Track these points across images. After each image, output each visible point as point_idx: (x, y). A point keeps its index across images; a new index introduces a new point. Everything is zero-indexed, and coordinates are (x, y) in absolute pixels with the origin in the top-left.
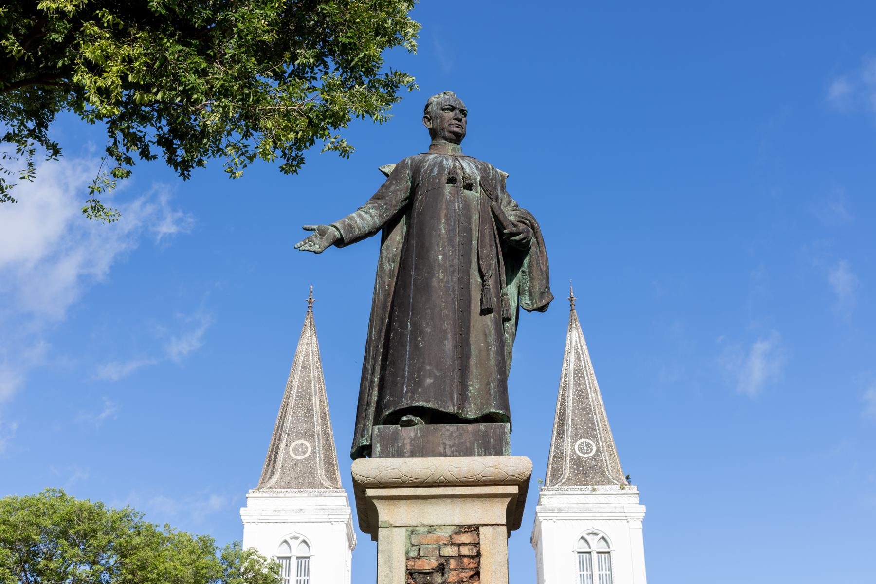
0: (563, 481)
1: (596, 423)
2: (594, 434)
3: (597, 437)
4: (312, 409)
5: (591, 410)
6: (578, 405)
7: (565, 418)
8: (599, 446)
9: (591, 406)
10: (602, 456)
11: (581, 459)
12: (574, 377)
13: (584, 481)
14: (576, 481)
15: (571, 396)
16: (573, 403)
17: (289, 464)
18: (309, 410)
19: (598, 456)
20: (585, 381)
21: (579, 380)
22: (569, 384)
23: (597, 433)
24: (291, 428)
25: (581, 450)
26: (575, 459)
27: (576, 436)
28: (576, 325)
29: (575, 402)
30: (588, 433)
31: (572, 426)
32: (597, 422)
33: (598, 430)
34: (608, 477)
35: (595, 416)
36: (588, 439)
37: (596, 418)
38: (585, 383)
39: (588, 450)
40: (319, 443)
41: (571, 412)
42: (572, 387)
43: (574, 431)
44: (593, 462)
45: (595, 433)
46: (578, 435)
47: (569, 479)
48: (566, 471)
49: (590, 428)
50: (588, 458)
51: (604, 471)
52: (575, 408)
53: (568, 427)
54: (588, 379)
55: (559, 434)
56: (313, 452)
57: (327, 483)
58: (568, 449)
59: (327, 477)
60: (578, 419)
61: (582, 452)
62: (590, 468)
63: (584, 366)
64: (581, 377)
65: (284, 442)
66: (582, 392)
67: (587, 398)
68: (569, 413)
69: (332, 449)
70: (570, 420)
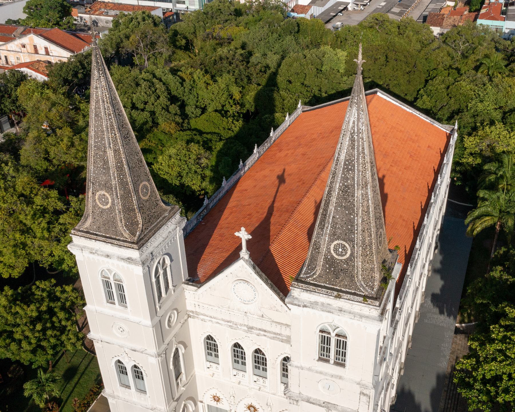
0: (315, 277)
3: (354, 241)
4: (108, 162)
5: (354, 210)
6: (342, 203)
9: (354, 206)
13: (333, 281)
16: (337, 199)
17: (97, 212)
18: (106, 162)
19: (351, 260)
20: (354, 175)
24: (94, 178)
25: (336, 250)
26: (329, 259)
27: (334, 236)
28: (357, 100)
32: (357, 225)
33: (357, 234)
34: (356, 283)
38: (353, 178)
40: (117, 194)
41: (333, 208)
47: (320, 276)
49: (348, 229)
50: (341, 260)
51: (354, 276)
52: (338, 204)
56: (113, 204)
57: (126, 234)
59: (126, 226)
60: (339, 218)
61: (336, 253)
62: (341, 270)
65: (91, 190)
66: (349, 189)
67: (352, 196)
69: (131, 195)
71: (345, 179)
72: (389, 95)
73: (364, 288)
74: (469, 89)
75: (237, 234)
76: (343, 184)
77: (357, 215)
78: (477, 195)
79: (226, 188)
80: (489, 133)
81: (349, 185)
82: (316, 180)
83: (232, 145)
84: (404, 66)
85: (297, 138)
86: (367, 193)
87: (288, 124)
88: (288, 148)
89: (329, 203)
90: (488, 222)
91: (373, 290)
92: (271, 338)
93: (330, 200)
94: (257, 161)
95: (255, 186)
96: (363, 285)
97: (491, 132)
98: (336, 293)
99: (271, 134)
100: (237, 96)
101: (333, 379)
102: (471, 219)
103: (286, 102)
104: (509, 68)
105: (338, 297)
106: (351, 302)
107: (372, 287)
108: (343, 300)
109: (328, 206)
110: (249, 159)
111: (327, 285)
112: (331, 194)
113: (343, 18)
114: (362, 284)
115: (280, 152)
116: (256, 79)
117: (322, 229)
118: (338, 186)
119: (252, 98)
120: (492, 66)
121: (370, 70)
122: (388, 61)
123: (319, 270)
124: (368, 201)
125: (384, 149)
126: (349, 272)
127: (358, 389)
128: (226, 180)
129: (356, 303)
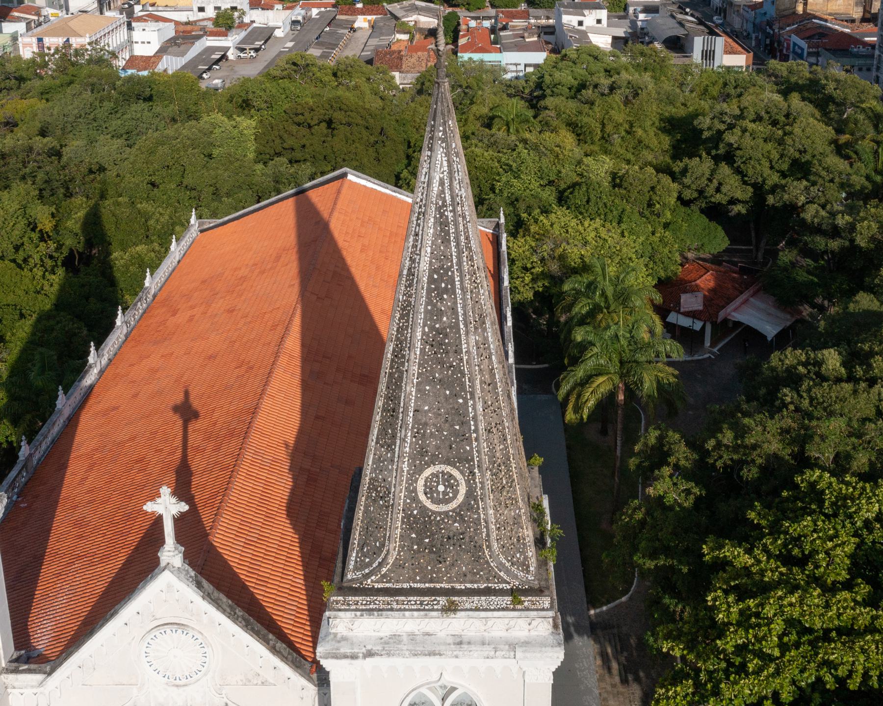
0: (384, 570)
1: (472, 423)
2: (465, 451)
5: (463, 387)
6: (432, 372)
7: (400, 397)
8: (475, 483)
10: (478, 508)
11: (430, 517)
12: (429, 291)
14: (413, 570)
15: (419, 345)
16: (420, 365)
20: (455, 303)
21: (442, 299)
23: (472, 448)
25: (432, 492)
29: (426, 362)
30: (451, 448)
31: (413, 427)
34: (487, 562)
35: (471, 403)
36: (448, 464)
37: (474, 409)
38: (454, 309)
39: (448, 494)
42: (420, 318)
43: (417, 441)
44: (456, 524)
45: (468, 448)
46: (426, 452)
48: (392, 546)
51: (481, 547)
52: (425, 378)
53: (403, 431)
54: (464, 299)
58: (401, 492)
60: (429, 410)
62: (449, 538)
63: (454, 262)
64: (446, 290)
66: (446, 336)
67: (456, 352)
68: (410, 394)
70: (411, 410)
71: (434, 314)
72: (369, 178)
73: (508, 572)
74: (489, 158)
76: (432, 328)
77: (473, 397)
78: (572, 338)
79: (67, 412)
80: (549, 227)
81: (445, 328)
82: (277, 355)
83: (52, 322)
84: (365, 133)
85: (204, 282)
86: (486, 339)
87: (177, 259)
88: (190, 304)
89: (401, 378)
90: (602, 385)
91: (528, 572)
93: (402, 373)
94: (123, 343)
95: (135, 396)
96: (503, 565)
97: (552, 225)
98: (443, 600)
99: (147, 283)
100: (47, 225)
102: (568, 387)
103: (151, 222)
104: (540, 118)
105: (451, 609)
106: (483, 614)
107: (523, 564)
108: (463, 613)
109: (399, 387)
110: (108, 339)
111: (419, 585)
112: (404, 356)
113: (220, 74)
114: (501, 563)
115: (174, 315)
116: (83, 188)
117: (390, 447)
118: (419, 335)
119: (78, 226)
120: (513, 119)
121: (304, 146)
122: (334, 129)
123: (393, 551)
124: (490, 358)
125: (389, 276)
126: (467, 539)
128: (65, 393)
129: (496, 614)
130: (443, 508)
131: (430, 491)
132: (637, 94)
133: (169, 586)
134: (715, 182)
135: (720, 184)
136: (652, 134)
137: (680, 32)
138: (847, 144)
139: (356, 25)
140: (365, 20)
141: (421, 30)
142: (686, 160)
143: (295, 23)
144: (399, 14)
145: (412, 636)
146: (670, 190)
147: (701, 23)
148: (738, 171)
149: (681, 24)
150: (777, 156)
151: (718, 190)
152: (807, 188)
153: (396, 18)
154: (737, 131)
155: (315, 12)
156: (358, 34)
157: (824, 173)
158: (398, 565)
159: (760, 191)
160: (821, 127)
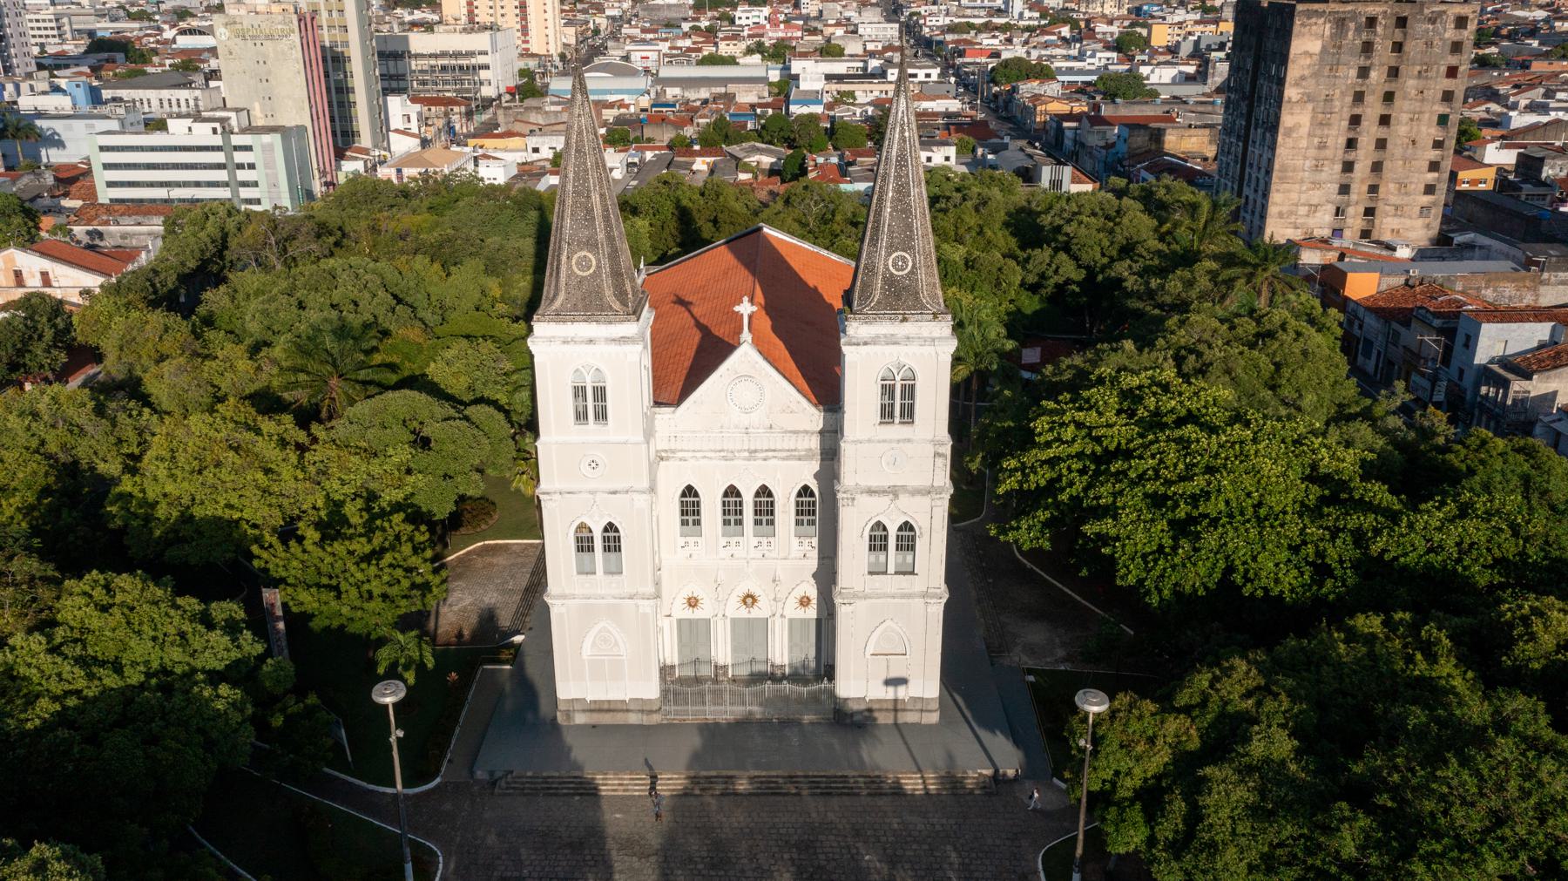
22: (889, 175)
55: (872, 239)
75: (737, 309)
92: (783, 459)
101: (901, 444)
117: (875, 246)
127: (930, 449)
130: (900, 273)
131: (895, 265)
132: (985, 203)
133: (746, 353)
134: (1054, 266)
135: (1058, 268)
136: (1000, 234)
137: (1028, 164)
138: (1169, 233)
139: (695, 167)
140: (703, 162)
141: (763, 171)
142: (1029, 251)
143: (630, 165)
144: (740, 155)
145: (885, 336)
146: (1016, 275)
147: (1049, 155)
148: (1076, 259)
149: (1030, 156)
150: (1108, 244)
151: (1056, 272)
152: (1130, 267)
153: (738, 159)
154: (1074, 224)
155: (649, 155)
156: (698, 176)
157: (1145, 254)
158: (879, 302)
159: (1091, 272)
160: (1145, 218)
